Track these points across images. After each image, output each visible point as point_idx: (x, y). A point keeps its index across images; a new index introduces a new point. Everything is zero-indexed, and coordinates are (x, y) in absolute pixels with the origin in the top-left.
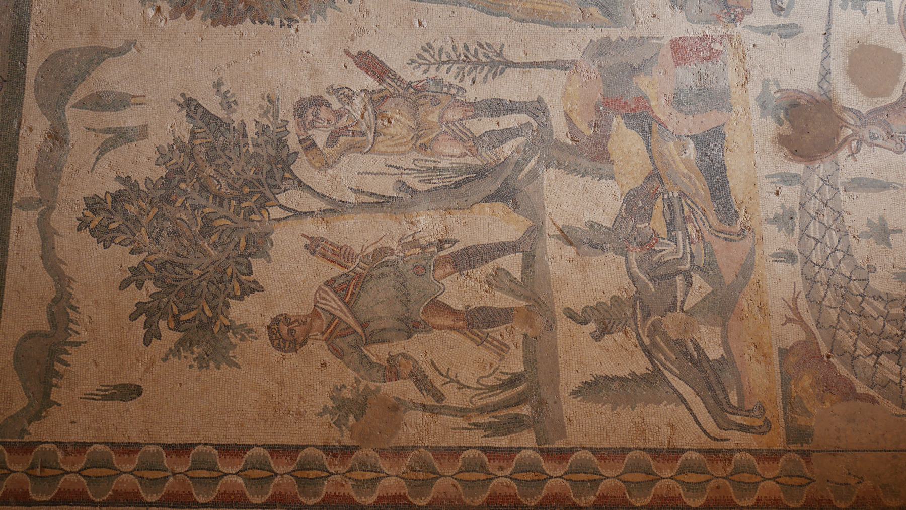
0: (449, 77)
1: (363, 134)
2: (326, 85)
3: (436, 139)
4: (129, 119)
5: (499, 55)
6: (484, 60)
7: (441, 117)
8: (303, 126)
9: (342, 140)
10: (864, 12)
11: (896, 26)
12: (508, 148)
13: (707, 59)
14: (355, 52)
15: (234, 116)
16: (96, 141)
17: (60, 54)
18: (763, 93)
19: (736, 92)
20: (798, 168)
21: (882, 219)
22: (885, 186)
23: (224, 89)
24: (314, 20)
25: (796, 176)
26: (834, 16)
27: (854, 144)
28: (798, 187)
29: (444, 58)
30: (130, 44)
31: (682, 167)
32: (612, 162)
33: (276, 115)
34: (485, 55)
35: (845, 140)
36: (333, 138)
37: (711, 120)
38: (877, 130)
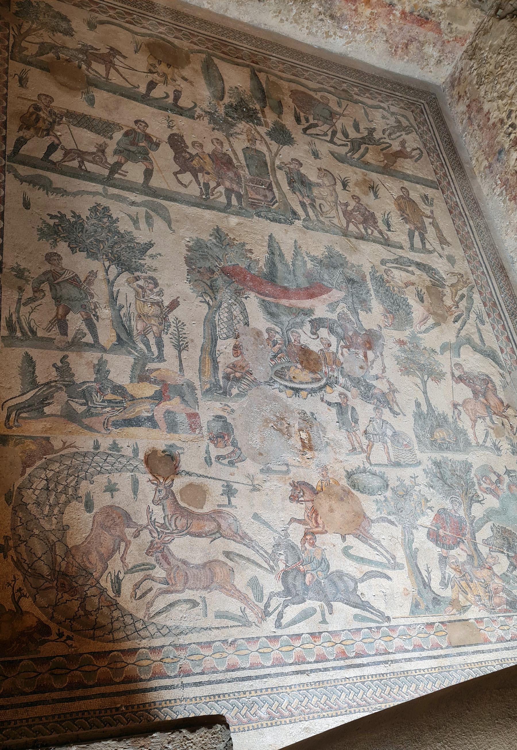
0: (171, 330)
1: (143, 297)
2: (164, 288)
3: (144, 321)
4: (143, 224)
5: (183, 349)
6: (181, 343)
7: (154, 325)
8: (145, 278)
9: (140, 290)
10: (222, 495)
11: (217, 508)
12: (141, 346)
13: (191, 427)
14: (178, 300)
15: (147, 258)
16: (133, 214)
17: (167, 210)
18: (177, 447)
19: (176, 436)
20: (141, 456)
21: (118, 490)
22: (135, 491)
23: (158, 256)
24: (191, 289)
25: (138, 455)
26: (218, 481)
27: (155, 482)
28: (132, 455)
29: (180, 330)
30: (174, 231)
31: (139, 409)
32: (138, 383)
33: (149, 270)
34: (183, 344)
35: (157, 478)
36: (140, 287)
37: (162, 423)
38: (163, 493)
